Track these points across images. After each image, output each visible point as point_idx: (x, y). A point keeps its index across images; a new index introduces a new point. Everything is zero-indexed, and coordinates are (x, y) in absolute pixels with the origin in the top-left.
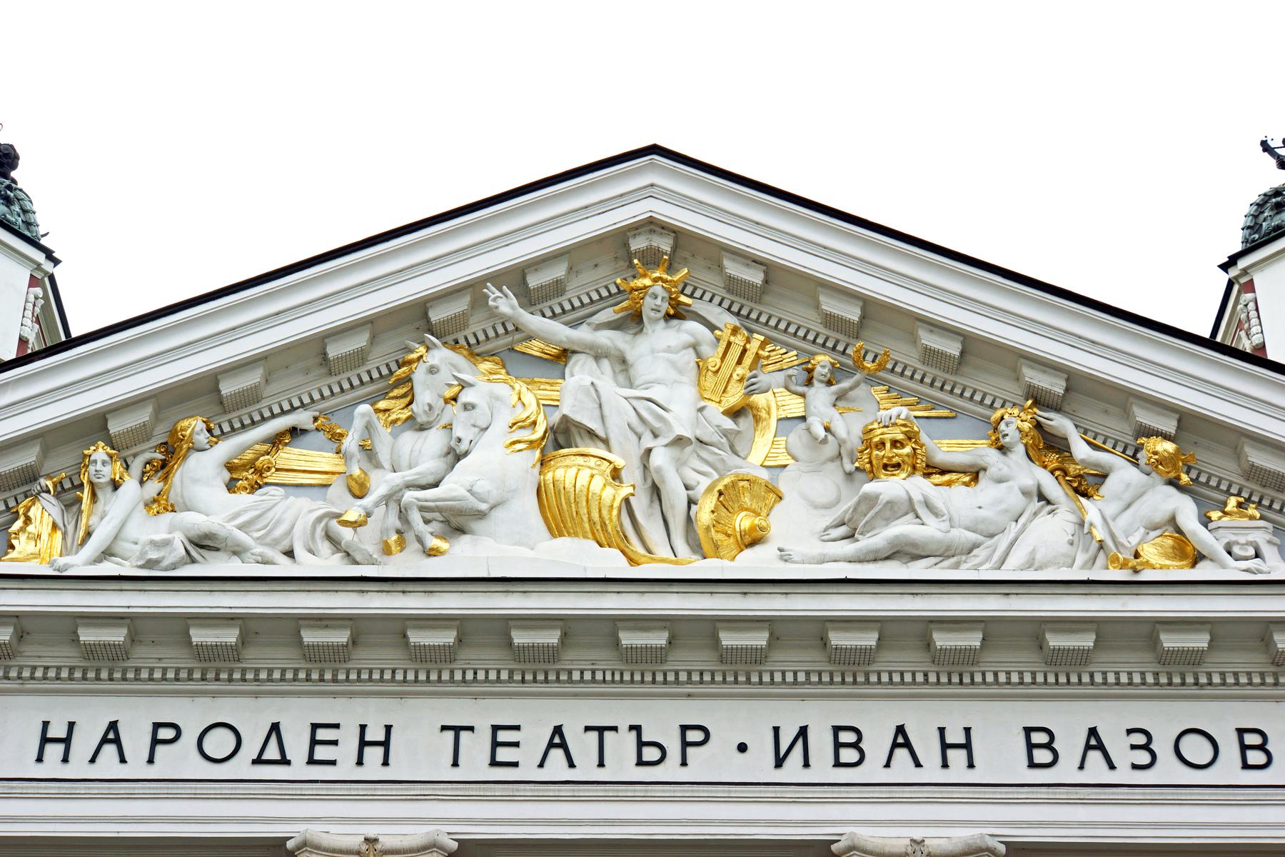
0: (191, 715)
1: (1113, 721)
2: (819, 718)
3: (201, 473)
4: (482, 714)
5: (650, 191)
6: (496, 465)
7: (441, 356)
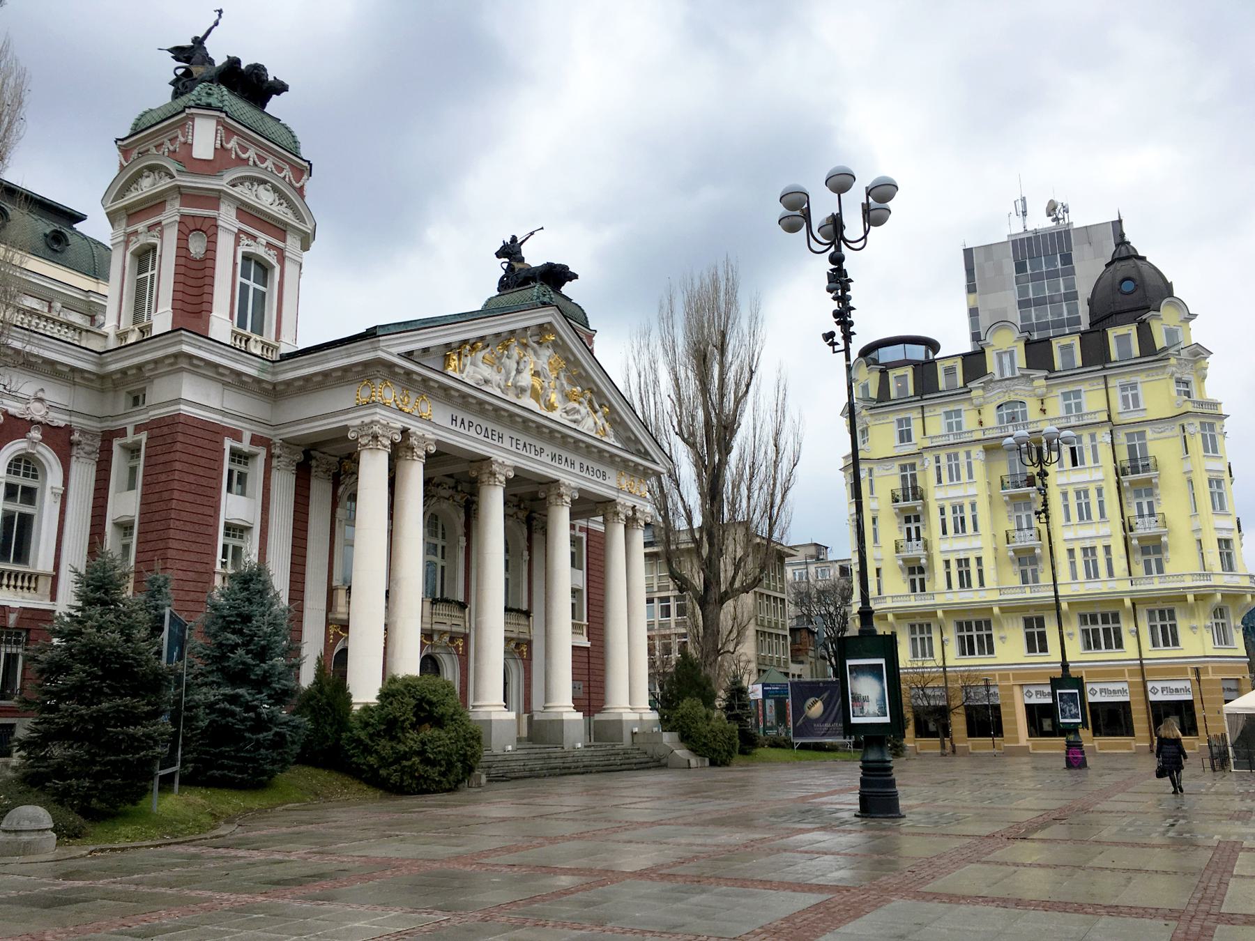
4: (516, 435)
5: (552, 315)
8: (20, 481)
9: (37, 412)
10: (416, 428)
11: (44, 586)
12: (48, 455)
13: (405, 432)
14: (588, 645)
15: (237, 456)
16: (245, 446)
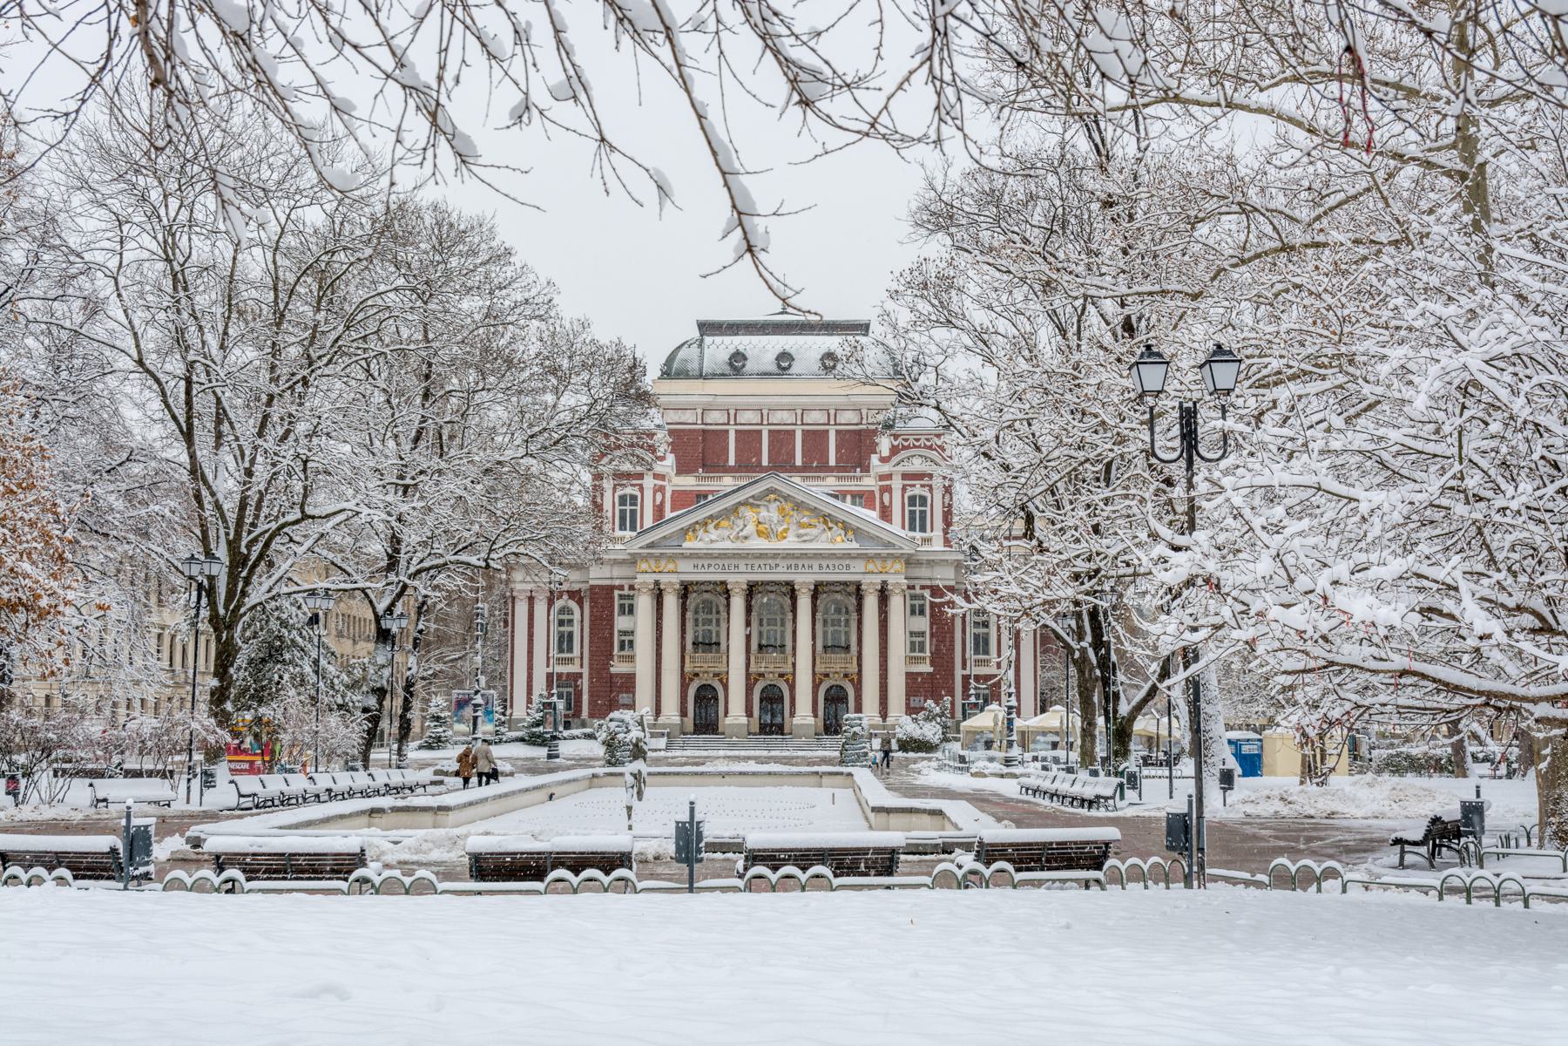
0: (713, 562)
1: (830, 563)
2: (793, 562)
3: (711, 527)
4: (750, 562)
6: (751, 528)
7: (742, 509)
8: (566, 617)
9: (565, 587)
10: (664, 579)
11: (577, 662)
12: (573, 605)
13: (657, 583)
14: (931, 670)
15: (621, 597)
16: (626, 592)
